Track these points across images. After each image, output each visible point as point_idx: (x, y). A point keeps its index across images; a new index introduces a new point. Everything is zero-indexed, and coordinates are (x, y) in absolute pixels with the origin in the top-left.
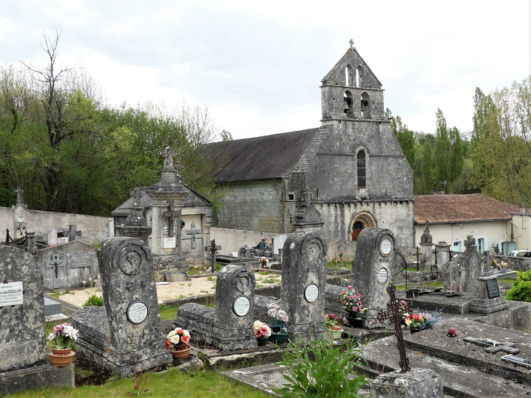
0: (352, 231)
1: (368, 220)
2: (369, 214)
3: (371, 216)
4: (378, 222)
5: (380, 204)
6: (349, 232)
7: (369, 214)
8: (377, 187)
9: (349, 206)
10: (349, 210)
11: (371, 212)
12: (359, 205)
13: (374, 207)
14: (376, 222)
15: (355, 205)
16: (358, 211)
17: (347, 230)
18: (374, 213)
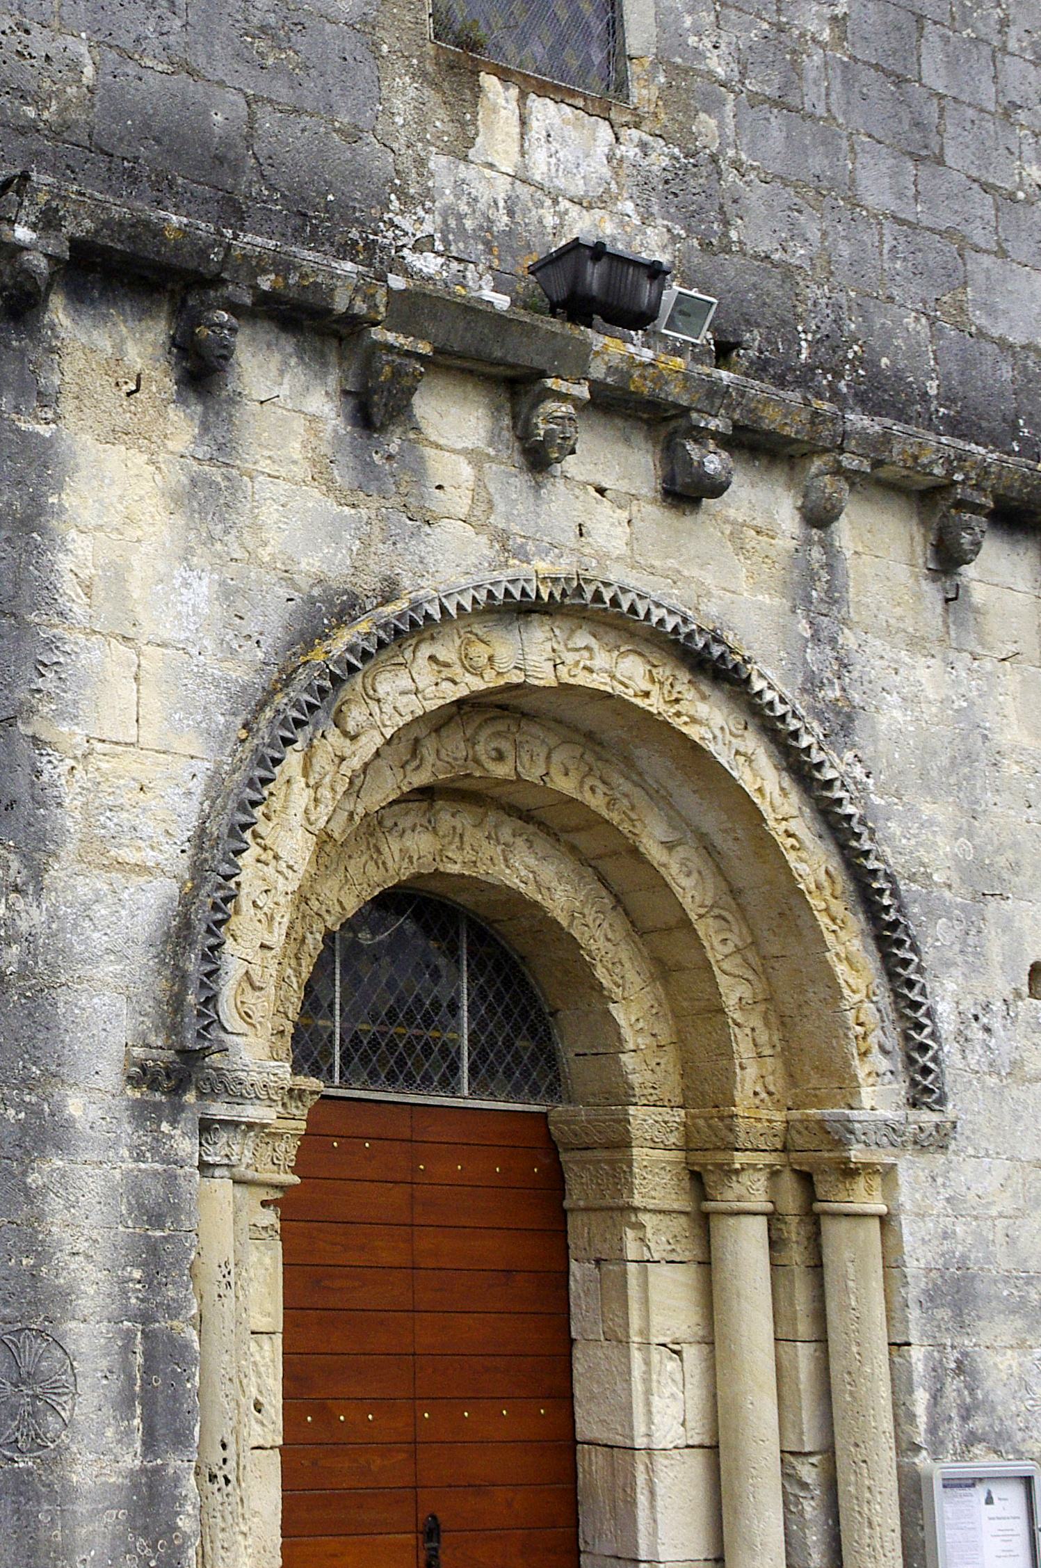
0: (255, 1048)
1: (690, 886)
2: (709, 720)
3: (762, 777)
4: (936, 939)
5: (947, 559)
6: (178, 1073)
7: (709, 720)
8: (876, 189)
9: (200, 373)
10: (209, 498)
11: (771, 679)
12: (454, 425)
13: (817, 590)
14: (888, 937)
15: (375, 409)
16: (450, 563)
17: (106, 1017)
18: (843, 722)
